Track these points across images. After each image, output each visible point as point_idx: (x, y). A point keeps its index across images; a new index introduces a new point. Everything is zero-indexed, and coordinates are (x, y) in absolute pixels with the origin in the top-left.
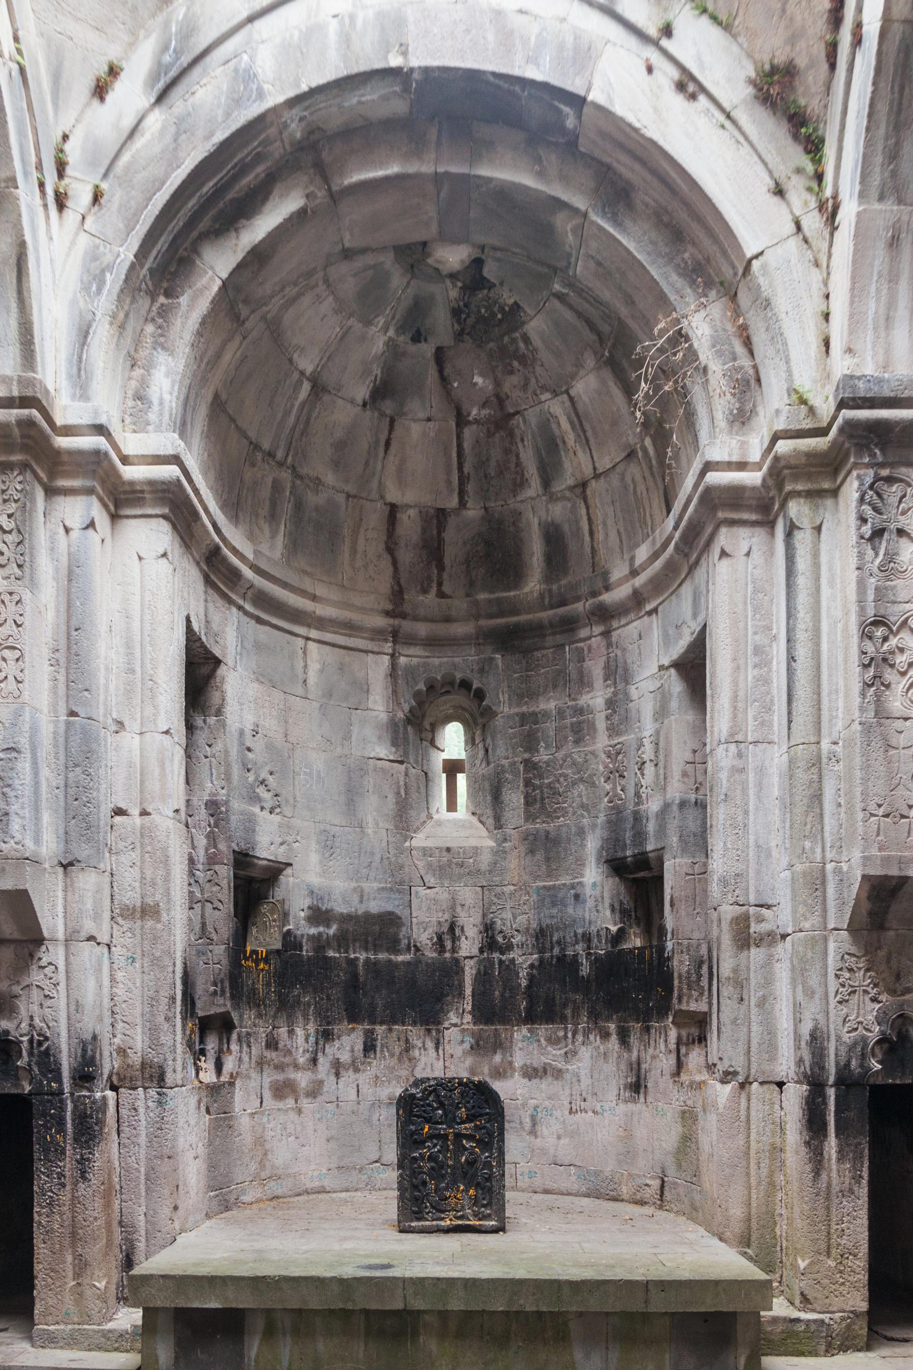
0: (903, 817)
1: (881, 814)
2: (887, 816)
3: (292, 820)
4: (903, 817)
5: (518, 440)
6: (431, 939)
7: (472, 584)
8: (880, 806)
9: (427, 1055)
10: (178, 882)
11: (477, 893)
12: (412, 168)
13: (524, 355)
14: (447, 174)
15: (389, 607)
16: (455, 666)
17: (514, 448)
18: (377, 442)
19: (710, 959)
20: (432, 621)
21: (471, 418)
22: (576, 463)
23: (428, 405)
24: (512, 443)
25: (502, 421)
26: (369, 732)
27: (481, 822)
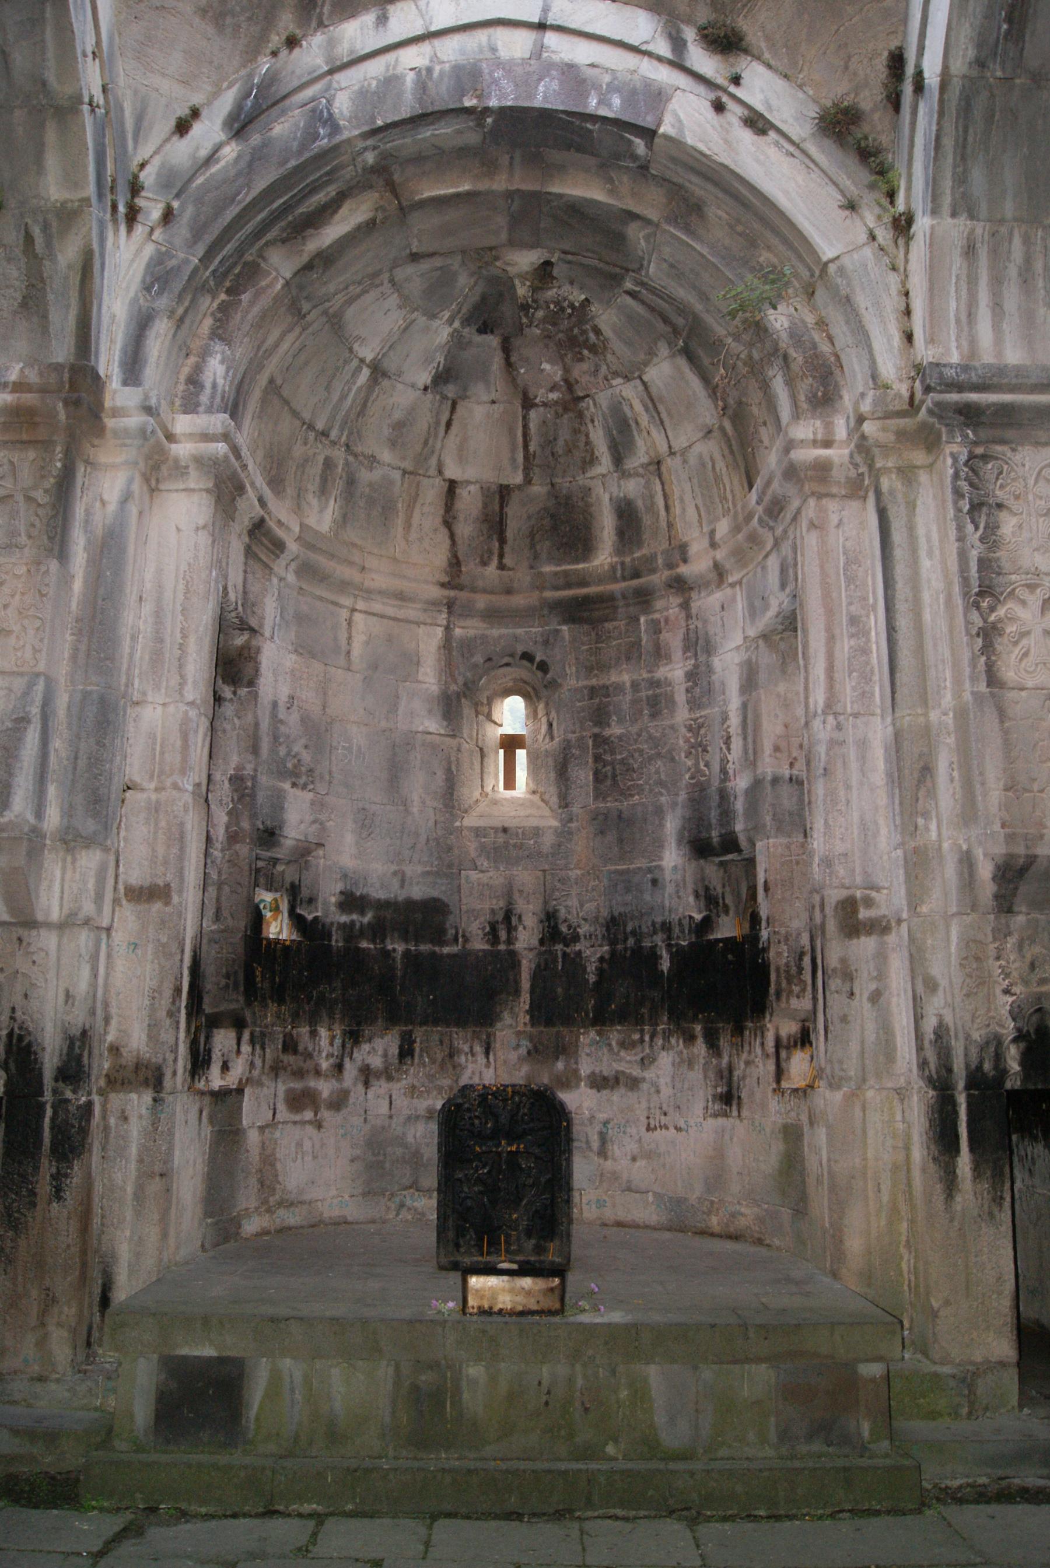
3: (327, 799)
4: (1026, 790)
5: (588, 421)
6: (483, 929)
7: (536, 557)
9: (475, 1062)
10: (193, 861)
11: (537, 878)
12: (483, 186)
13: (594, 345)
14: (518, 190)
15: (447, 579)
16: (516, 638)
17: (583, 428)
18: (437, 423)
19: (813, 949)
20: (492, 593)
21: (537, 401)
23: (493, 389)
25: (572, 401)
26: (418, 705)
27: (543, 800)
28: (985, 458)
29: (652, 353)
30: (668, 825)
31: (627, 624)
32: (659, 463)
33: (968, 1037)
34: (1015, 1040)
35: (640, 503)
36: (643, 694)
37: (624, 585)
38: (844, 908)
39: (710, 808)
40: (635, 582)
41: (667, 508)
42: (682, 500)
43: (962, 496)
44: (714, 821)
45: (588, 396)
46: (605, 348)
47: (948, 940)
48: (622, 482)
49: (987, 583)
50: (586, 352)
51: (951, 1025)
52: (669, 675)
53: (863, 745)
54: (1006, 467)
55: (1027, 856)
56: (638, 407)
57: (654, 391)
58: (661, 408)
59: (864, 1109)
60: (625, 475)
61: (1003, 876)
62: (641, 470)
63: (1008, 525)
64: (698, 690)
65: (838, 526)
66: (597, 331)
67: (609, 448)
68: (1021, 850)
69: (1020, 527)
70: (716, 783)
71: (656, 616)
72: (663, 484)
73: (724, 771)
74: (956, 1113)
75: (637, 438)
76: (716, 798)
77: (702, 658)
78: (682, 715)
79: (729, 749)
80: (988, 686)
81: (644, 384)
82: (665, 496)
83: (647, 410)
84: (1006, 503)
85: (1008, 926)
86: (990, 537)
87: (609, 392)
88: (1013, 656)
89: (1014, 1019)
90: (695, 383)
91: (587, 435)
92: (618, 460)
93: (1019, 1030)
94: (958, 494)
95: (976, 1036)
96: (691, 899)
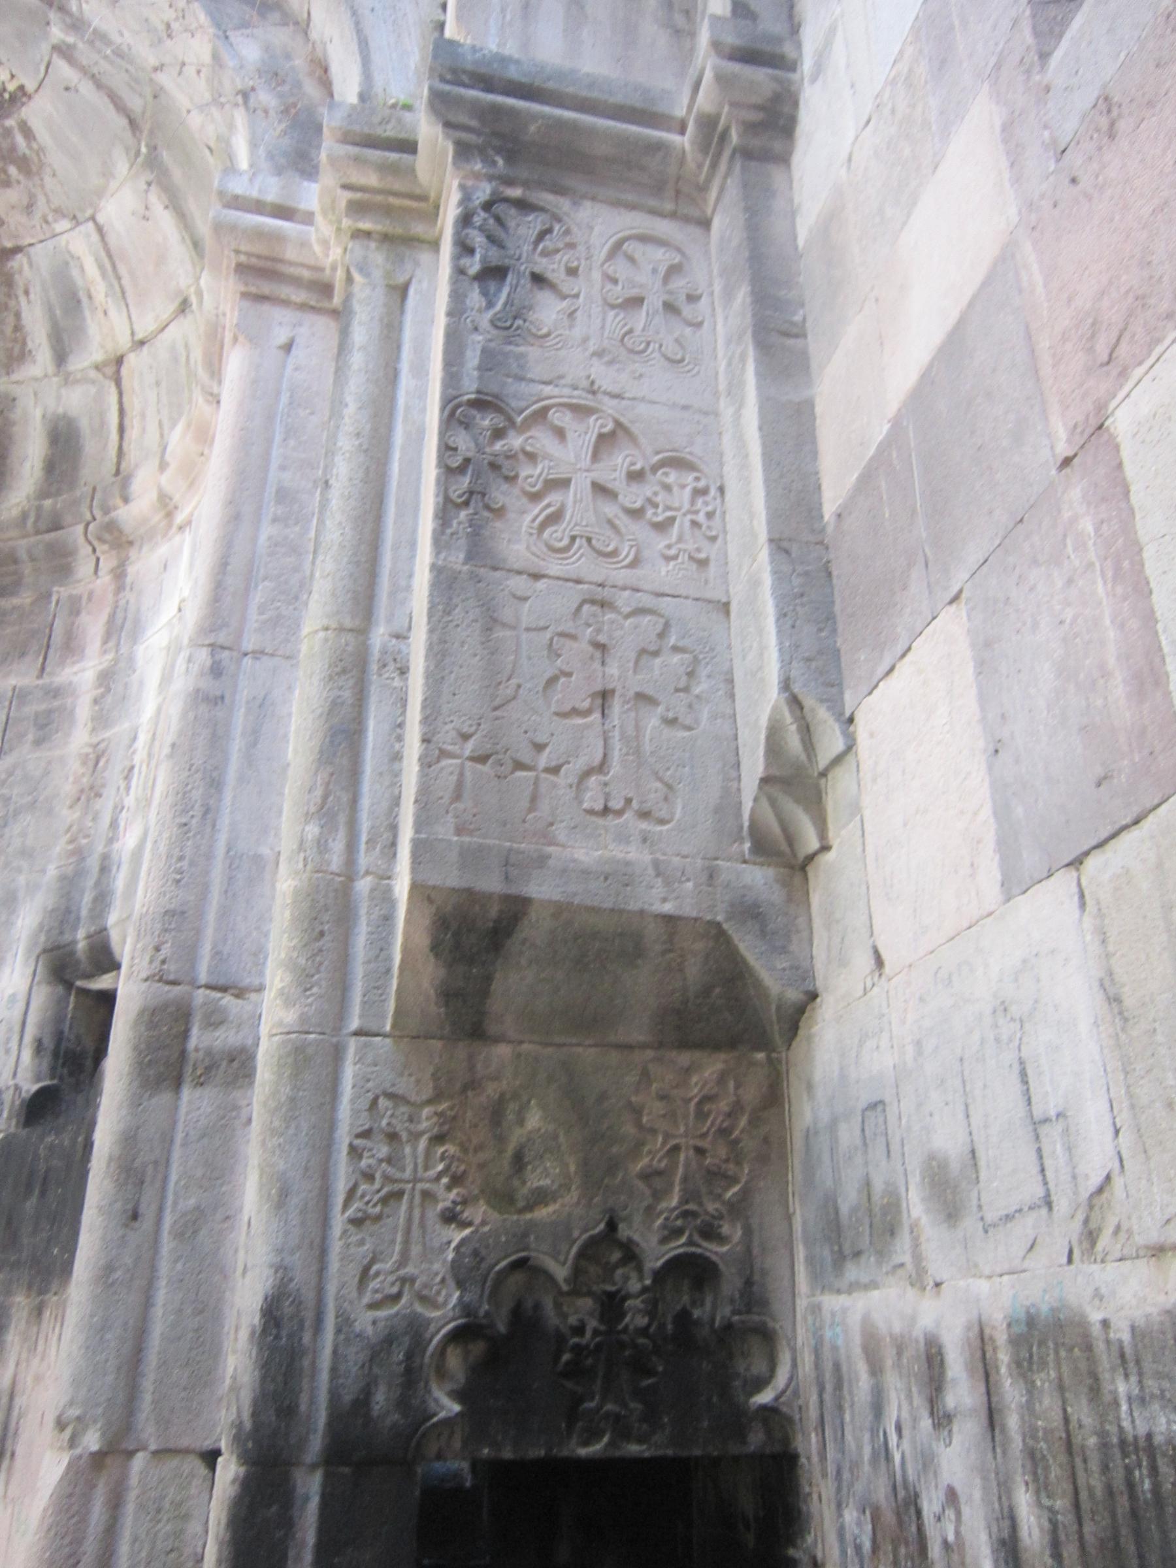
0: (519, 766)
1: (467, 753)
2: (482, 759)
4: (519, 766)
5: (20, 292)
8: (466, 737)
17: (12, 303)
22: (106, 330)
24: (9, 296)
28: (523, 205)
29: (107, 173)
30: (19, 923)
31: (32, 604)
32: (119, 361)
33: (344, 1322)
34: (459, 1336)
35: (84, 424)
36: (30, 710)
37: (33, 539)
38: (152, 1025)
39: (82, 893)
40: (48, 537)
41: (121, 429)
42: (143, 416)
43: (470, 251)
44: (84, 913)
45: (17, 250)
46: (41, 165)
47: (333, 1090)
48: (63, 391)
49: (494, 388)
50: (13, 170)
51: (309, 1296)
52: (75, 679)
53: (262, 707)
54: (557, 227)
55: (507, 898)
56: (92, 270)
57: (112, 241)
58: (122, 270)
59: (116, 1504)
60: (68, 380)
61: (457, 946)
62: (93, 374)
63: (547, 311)
64: (109, 699)
65: (288, 347)
66: (28, 133)
67: (49, 336)
68: (491, 883)
69: (571, 315)
70: (100, 848)
71: (79, 589)
72: (120, 394)
73: (114, 824)
74: (287, 1523)
75: (89, 321)
76: (95, 870)
77: (124, 650)
78: (79, 738)
79: (128, 789)
80: (469, 558)
81: (100, 230)
82: (122, 412)
83: (104, 274)
84: (549, 275)
85: (472, 1068)
86: (512, 324)
87: (50, 244)
88: (528, 518)
89: (460, 1284)
90: (165, 220)
91: (18, 315)
92: (61, 358)
93: (466, 1309)
94: (464, 248)
95: (366, 1322)
96: (27, 1056)
